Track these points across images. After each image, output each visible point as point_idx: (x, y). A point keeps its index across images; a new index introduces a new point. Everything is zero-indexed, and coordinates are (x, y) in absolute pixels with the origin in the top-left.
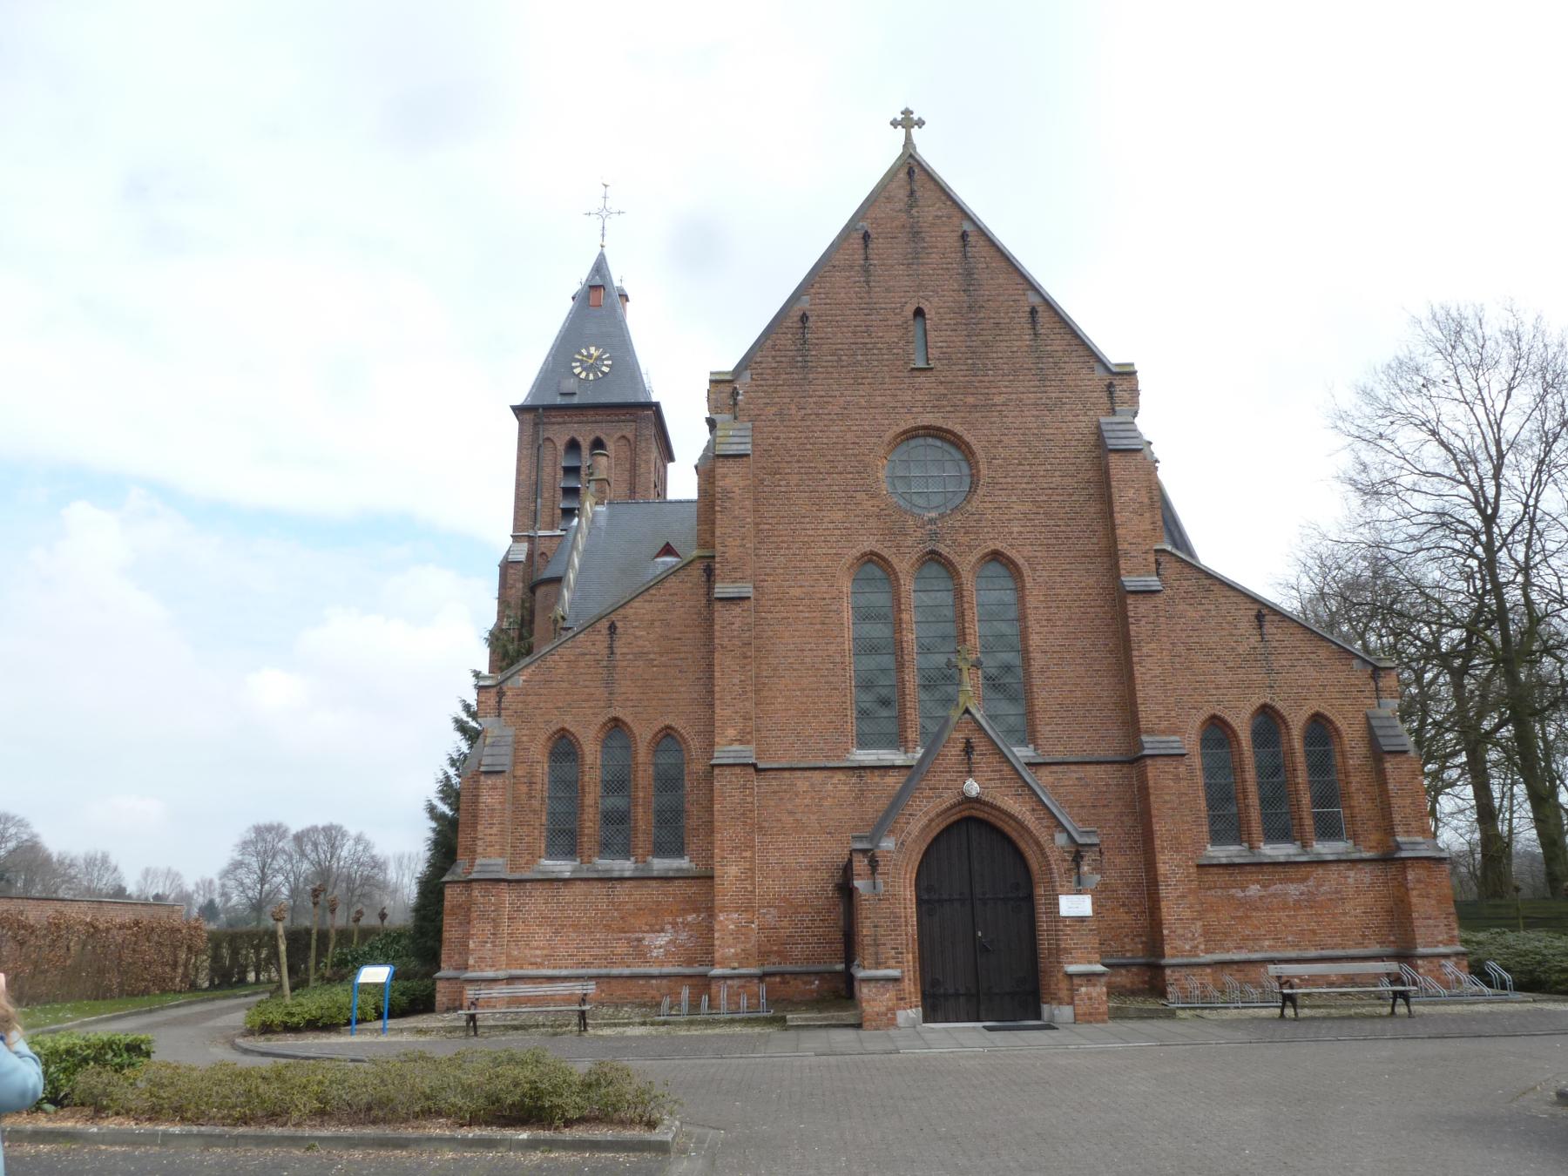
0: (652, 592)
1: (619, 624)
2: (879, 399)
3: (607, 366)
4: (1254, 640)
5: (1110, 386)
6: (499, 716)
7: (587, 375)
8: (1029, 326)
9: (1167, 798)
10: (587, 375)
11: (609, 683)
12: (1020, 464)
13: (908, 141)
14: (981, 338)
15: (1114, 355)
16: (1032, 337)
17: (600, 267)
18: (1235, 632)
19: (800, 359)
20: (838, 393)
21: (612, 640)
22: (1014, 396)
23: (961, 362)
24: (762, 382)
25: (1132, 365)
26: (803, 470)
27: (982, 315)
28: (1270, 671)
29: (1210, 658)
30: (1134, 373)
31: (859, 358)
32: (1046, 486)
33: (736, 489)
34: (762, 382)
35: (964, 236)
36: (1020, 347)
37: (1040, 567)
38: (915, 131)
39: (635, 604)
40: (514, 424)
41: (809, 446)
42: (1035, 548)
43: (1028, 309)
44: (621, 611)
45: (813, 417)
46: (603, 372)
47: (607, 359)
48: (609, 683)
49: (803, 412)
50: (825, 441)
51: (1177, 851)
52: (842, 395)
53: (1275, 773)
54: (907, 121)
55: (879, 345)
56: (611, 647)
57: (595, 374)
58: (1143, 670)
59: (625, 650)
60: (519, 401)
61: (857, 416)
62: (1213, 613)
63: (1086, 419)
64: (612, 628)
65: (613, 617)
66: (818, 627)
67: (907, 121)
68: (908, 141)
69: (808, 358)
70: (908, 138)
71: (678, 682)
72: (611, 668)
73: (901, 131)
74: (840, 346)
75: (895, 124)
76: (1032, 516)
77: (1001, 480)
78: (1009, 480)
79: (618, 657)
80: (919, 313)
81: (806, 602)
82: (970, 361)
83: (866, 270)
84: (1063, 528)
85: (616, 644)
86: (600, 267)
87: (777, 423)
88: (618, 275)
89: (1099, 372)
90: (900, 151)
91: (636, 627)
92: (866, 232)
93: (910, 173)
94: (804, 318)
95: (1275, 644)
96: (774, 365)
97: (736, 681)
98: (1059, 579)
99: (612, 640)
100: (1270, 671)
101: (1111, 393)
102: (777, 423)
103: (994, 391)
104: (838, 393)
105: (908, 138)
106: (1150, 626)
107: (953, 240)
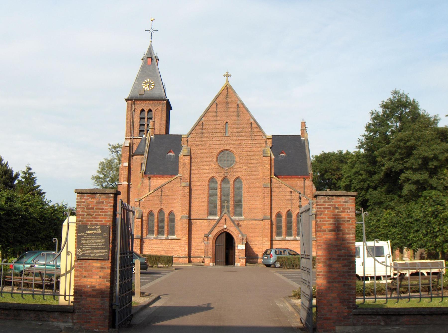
0: (169, 183)
1: (163, 189)
2: (217, 143)
3: (153, 86)
4: (289, 197)
5: (266, 141)
6: (139, 207)
8: (250, 127)
9: (266, 228)
11: (161, 202)
13: (228, 81)
16: (250, 129)
17: (150, 50)
18: (286, 195)
19: (201, 133)
20: (209, 141)
21: (162, 192)
22: (246, 143)
23: (235, 135)
26: (201, 158)
27: (240, 124)
28: (292, 203)
29: (280, 200)
33: (187, 163)
36: (247, 132)
37: (248, 180)
38: (229, 78)
39: (166, 185)
40: (125, 103)
44: (163, 187)
47: (153, 83)
48: (161, 202)
49: (201, 145)
51: (267, 238)
53: (289, 222)
54: (227, 75)
55: (218, 130)
56: (161, 194)
58: (265, 203)
59: (164, 195)
60: (126, 98)
61: (212, 146)
62: (282, 191)
63: (260, 148)
64: (162, 190)
65: (161, 188)
66: (202, 191)
67: (227, 75)
68: (228, 81)
69: (203, 133)
70: (227, 79)
72: (161, 199)
74: (209, 130)
75: (225, 76)
76: (247, 169)
77: (242, 162)
78: (243, 161)
79: (162, 196)
80: (227, 122)
81: (200, 186)
83: (216, 112)
84: (253, 172)
85: (162, 193)
86: (150, 50)
87: (196, 147)
88: (156, 51)
89: (264, 138)
94: (203, 123)
95: (293, 197)
96: (196, 134)
97: (186, 203)
98: (251, 183)
99: (162, 192)
100: (292, 203)
101: (266, 143)
102: (196, 147)
103: (241, 141)
104: (209, 141)
105: (227, 79)
106: (267, 194)
107: (235, 106)
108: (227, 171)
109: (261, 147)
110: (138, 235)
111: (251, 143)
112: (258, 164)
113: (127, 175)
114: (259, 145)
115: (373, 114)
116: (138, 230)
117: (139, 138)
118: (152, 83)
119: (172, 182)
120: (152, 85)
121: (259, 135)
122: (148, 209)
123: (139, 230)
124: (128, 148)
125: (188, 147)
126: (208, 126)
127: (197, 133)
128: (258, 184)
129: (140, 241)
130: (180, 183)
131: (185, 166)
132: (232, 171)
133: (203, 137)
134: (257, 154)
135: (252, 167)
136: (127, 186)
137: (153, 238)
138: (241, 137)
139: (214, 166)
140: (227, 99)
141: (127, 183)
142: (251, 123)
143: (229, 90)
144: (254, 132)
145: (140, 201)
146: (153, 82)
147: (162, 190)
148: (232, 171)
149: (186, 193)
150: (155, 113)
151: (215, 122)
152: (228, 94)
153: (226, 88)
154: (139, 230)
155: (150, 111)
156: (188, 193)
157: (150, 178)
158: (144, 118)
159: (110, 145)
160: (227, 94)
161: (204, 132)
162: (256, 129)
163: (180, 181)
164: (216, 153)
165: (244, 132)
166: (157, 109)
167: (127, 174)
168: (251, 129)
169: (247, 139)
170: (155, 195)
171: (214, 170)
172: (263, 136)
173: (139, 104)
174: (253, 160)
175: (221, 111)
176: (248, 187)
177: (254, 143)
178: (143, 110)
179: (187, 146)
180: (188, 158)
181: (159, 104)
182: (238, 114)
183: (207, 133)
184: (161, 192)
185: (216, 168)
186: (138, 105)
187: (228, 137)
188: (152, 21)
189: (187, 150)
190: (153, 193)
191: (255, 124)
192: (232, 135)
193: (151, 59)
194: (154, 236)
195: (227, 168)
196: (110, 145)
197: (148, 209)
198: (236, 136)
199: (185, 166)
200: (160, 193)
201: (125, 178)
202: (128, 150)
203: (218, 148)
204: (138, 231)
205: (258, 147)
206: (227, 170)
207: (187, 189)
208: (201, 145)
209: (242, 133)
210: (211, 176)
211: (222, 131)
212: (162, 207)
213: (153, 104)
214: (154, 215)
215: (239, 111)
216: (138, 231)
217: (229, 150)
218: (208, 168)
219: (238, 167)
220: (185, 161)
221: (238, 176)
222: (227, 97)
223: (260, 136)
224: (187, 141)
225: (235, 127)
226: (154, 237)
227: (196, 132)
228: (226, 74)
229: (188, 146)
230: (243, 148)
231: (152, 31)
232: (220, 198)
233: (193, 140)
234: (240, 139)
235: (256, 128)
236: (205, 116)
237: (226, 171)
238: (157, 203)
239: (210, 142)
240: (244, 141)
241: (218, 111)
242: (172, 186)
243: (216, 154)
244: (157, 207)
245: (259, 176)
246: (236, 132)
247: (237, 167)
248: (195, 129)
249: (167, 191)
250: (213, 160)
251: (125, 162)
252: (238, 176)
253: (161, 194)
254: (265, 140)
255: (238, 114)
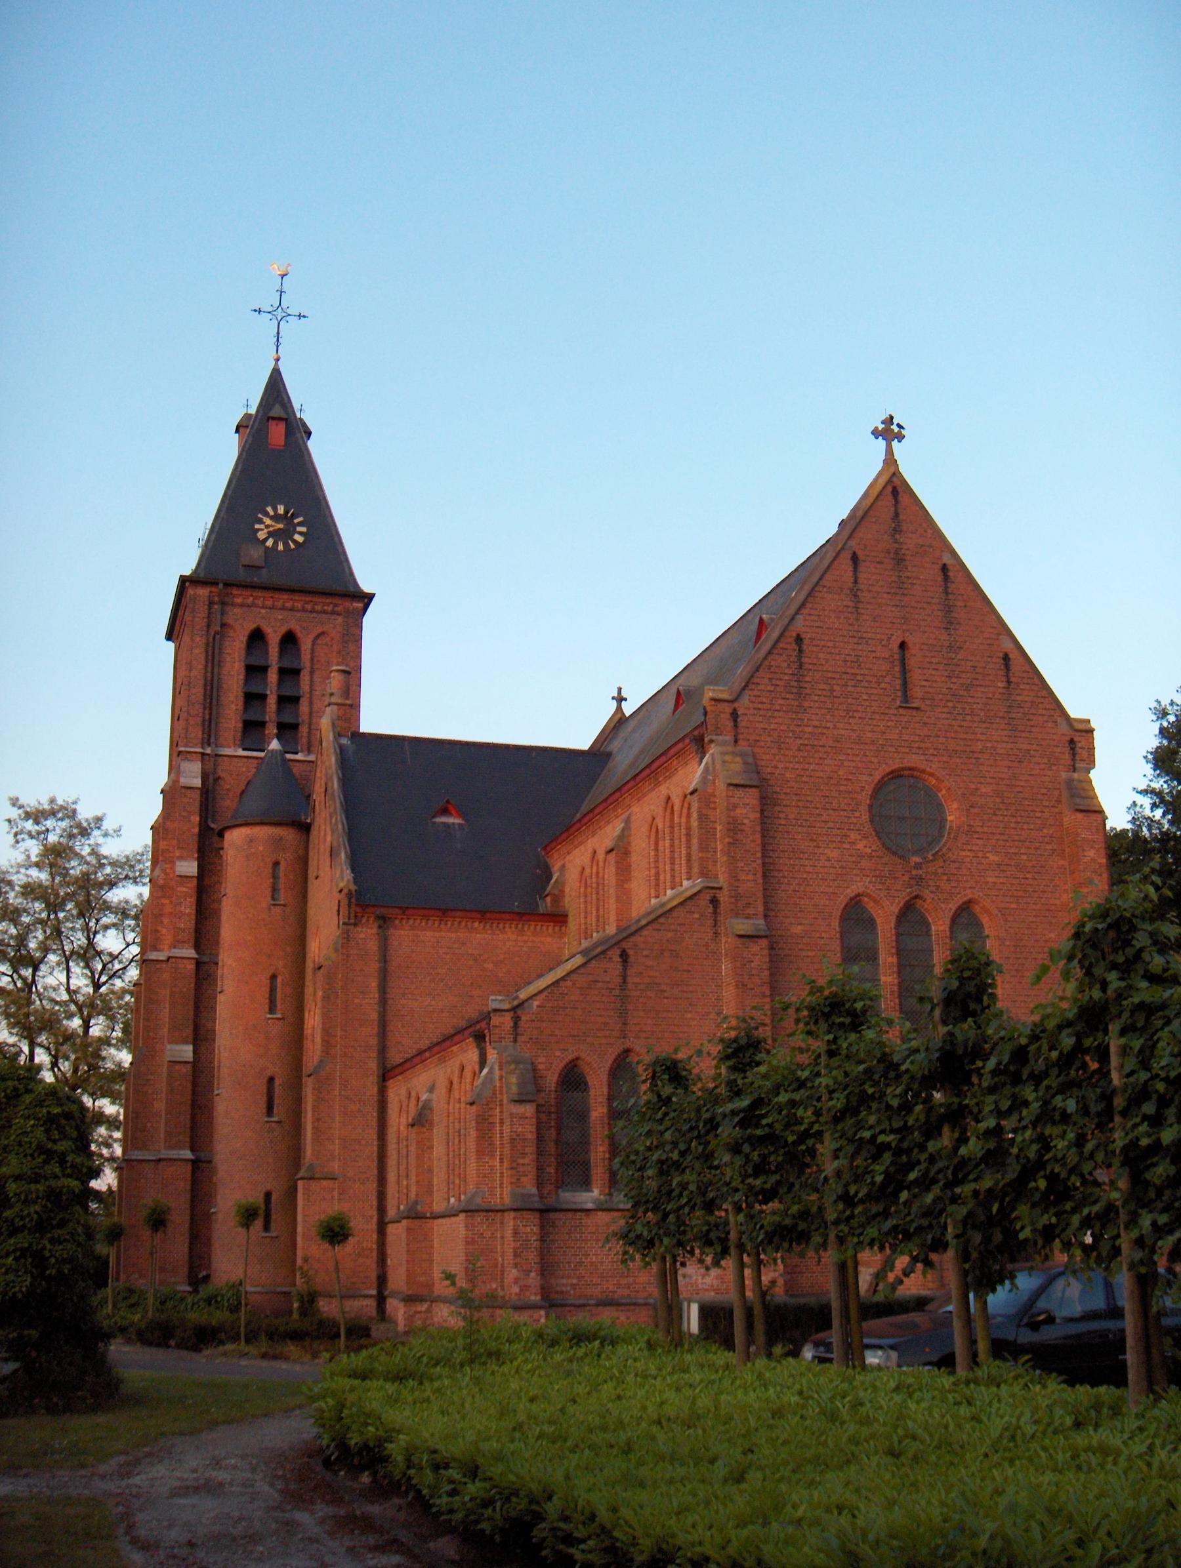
0: (662, 920)
1: (631, 952)
2: (869, 735)
3: (301, 533)
5: (1072, 741)
6: (515, 1041)
7: (276, 543)
10: (276, 543)
11: (623, 1014)
12: (995, 814)
13: (890, 460)
14: (961, 681)
15: (1074, 711)
17: (275, 388)
21: (625, 969)
22: (989, 745)
24: (760, 706)
25: (1088, 721)
26: (800, 804)
27: (960, 656)
30: (1091, 731)
31: (849, 689)
32: (1016, 838)
33: (746, 821)
34: (760, 706)
35: (944, 568)
39: (645, 932)
41: (804, 779)
42: (1007, 899)
43: (1001, 655)
44: (632, 939)
45: (808, 748)
46: (295, 542)
48: (623, 1014)
49: (799, 742)
50: (821, 774)
52: (835, 727)
54: (889, 432)
55: (868, 678)
56: (624, 977)
57: (286, 545)
59: (636, 980)
61: (849, 751)
63: (1049, 773)
64: (624, 956)
65: (624, 945)
67: (889, 432)
68: (890, 460)
70: (889, 451)
71: (689, 1015)
73: (881, 443)
74: (830, 675)
75: (876, 433)
76: (1005, 868)
77: (978, 829)
78: (985, 829)
79: (630, 986)
82: (950, 704)
84: (1030, 881)
85: (629, 972)
86: (275, 388)
90: (879, 466)
91: (647, 956)
92: (854, 553)
93: (895, 492)
94: (799, 639)
96: (772, 688)
99: (625, 969)
101: (1073, 749)
103: (972, 737)
105: (889, 451)
107: (935, 573)
108: (920, 872)
109: (1054, 768)
110: (521, 1191)
111: (1010, 746)
112: (1049, 847)
113: (193, 917)
114: (1045, 760)
115: (1164, 714)
116: (521, 1161)
117: (241, 752)
118: (296, 521)
119: (675, 914)
120: (300, 529)
121: (1041, 712)
122: (558, 1053)
123: (526, 1161)
124: (197, 796)
125: (738, 748)
126: (821, 655)
127: (774, 682)
128: (1053, 935)
129: (537, 1221)
130: (710, 922)
131: (739, 836)
132: (940, 871)
133: (806, 704)
134: (1040, 797)
135: (1024, 857)
136: (191, 966)
137: (590, 1206)
138: (968, 718)
139: (860, 845)
140: (897, 536)
141: (191, 953)
142: (1006, 658)
143: (903, 498)
144: (1018, 698)
145: (519, 1012)
146: (301, 519)
147: (624, 956)
148: (940, 871)
149: (754, 972)
150: (313, 650)
151: (855, 640)
152: (901, 517)
153: (890, 489)
154: (526, 1161)
155: (289, 640)
156: (767, 973)
157: (384, 921)
158: (264, 669)
159: (15, 802)
160: (897, 515)
161: (807, 679)
162: (1027, 687)
163: (711, 910)
164: (867, 782)
165: (980, 695)
166: (323, 633)
167: (194, 912)
168: (1009, 682)
169: (994, 726)
170: (591, 978)
171: (864, 863)
172: (1059, 720)
173: (242, 605)
174: (1025, 826)
175: (874, 589)
176: (1012, 949)
177: (1021, 746)
178: (257, 637)
179: (736, 741)
180: (750, 798)
181: (333, 613)
182: (948, 609)
183: (822, 686)
184: (619, 966)
185: (871, 857)
186: (237, 610)
187: (914, 713)
188: (283, 276)
189: (738, 759)
190: (582, 970)
191: (1022, 660)
192: (928, 702)
193: (282, 426)
194: (596, 1192)
195: (917, 859)
196: (15, 802)
197: (558, 1053)
198: (945, 710)
199: (739, 836)
200: (617, 973)
201: (183, 931)
202: (197, 804)
203: (876, 761)
204: (521, 1169)
205: (1043, 766)
206: (918, 866)
207: (758, 952)
208: (799, 742)
209: (970, 700)
210: (851, 892)
211: (887, 680)
212: (628, 1044)
213: (304, 610)
214: (586, 1084)
215: (950, 596)
216: (521, 1169)
217: (923, 771)
218: (835, 854)
219: (968, 854)
220: (738, 811)
221: (969, 894)
222: (895, 530)
223: (1045, 718)
224: (734, 715)
225: (941, 667)
226: (595, 1201)
227: (769, 676)
228: (881, 427)
229: (741, 742)
230: (981, 768)
231: (279, 314)
232: (897, 1001)
233: (761, 712)
234: (965, 724)
235: (1025, 681)
236: (809, 605)
237: (914, 872)
238: (606, 1024)
239: (835, 732)
240: (983, 737)
241: (861, 587)
242: (670, 934)
243: (869, 790)
244: (604, 1041)
245: (1058, 902)
246: (945, 691)
247: (963, 853)
248: (766, 663)
249: (650, 963)
250: (857, 814)
251: (181, 858)
252: (970, 896)
253: (624, 977)
254: (1068, 738)
255: (948, 609)
